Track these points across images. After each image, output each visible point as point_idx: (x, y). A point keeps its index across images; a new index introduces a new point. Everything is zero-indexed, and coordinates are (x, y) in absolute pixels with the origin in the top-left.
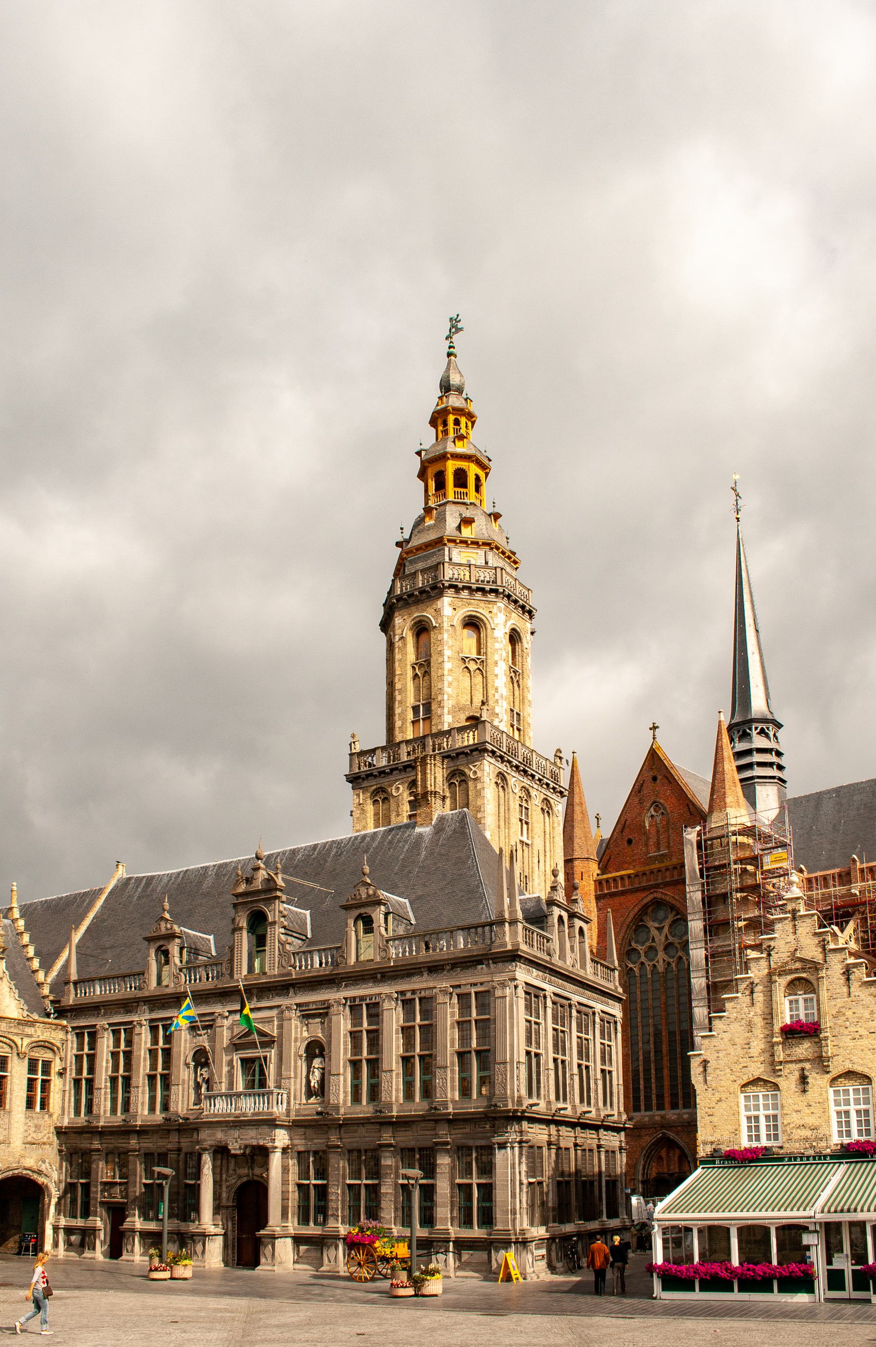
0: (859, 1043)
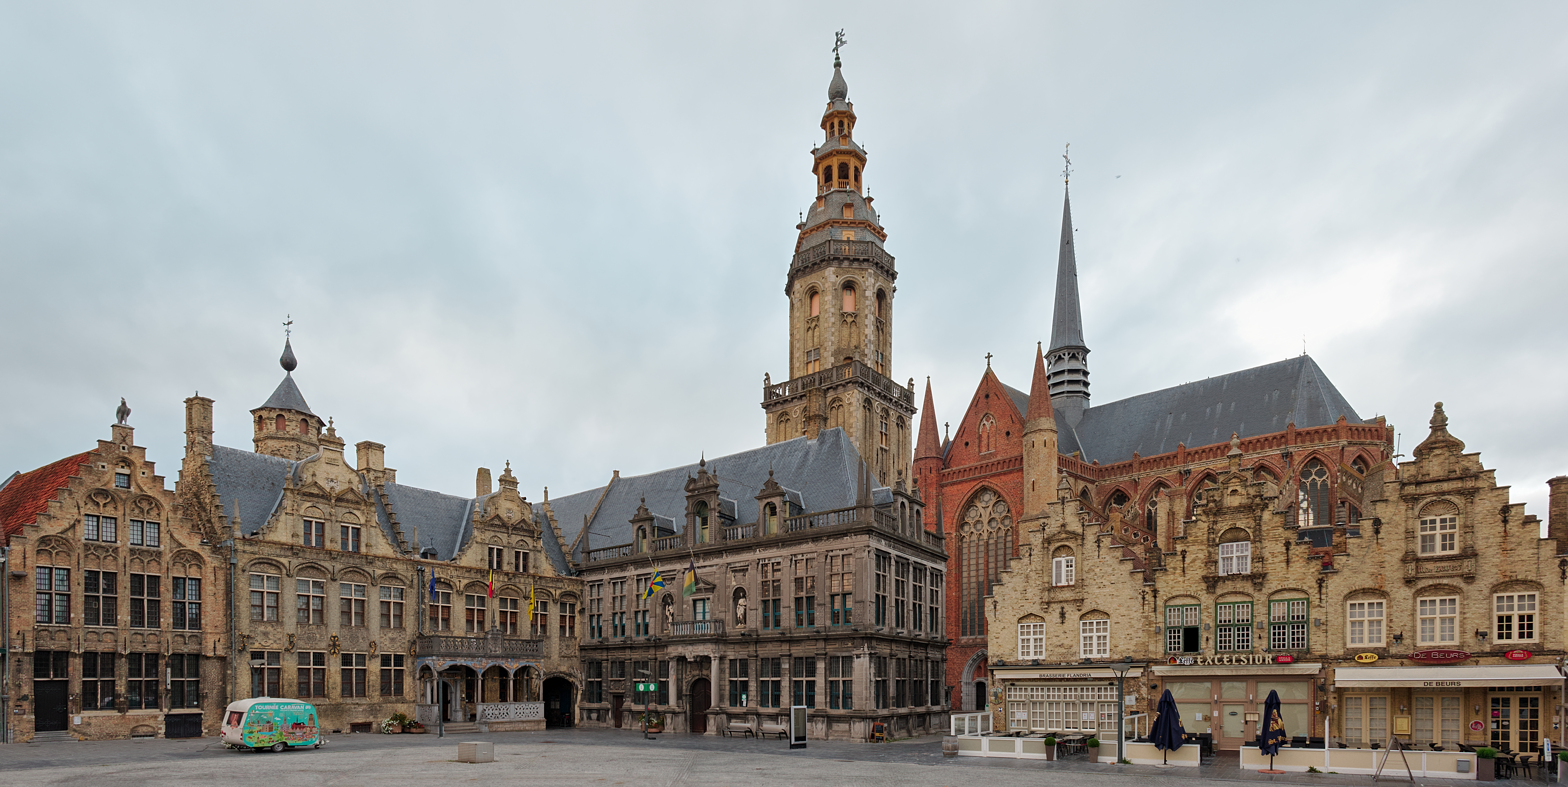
0: (1104, 590)
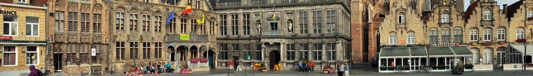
0: (413, 25)
